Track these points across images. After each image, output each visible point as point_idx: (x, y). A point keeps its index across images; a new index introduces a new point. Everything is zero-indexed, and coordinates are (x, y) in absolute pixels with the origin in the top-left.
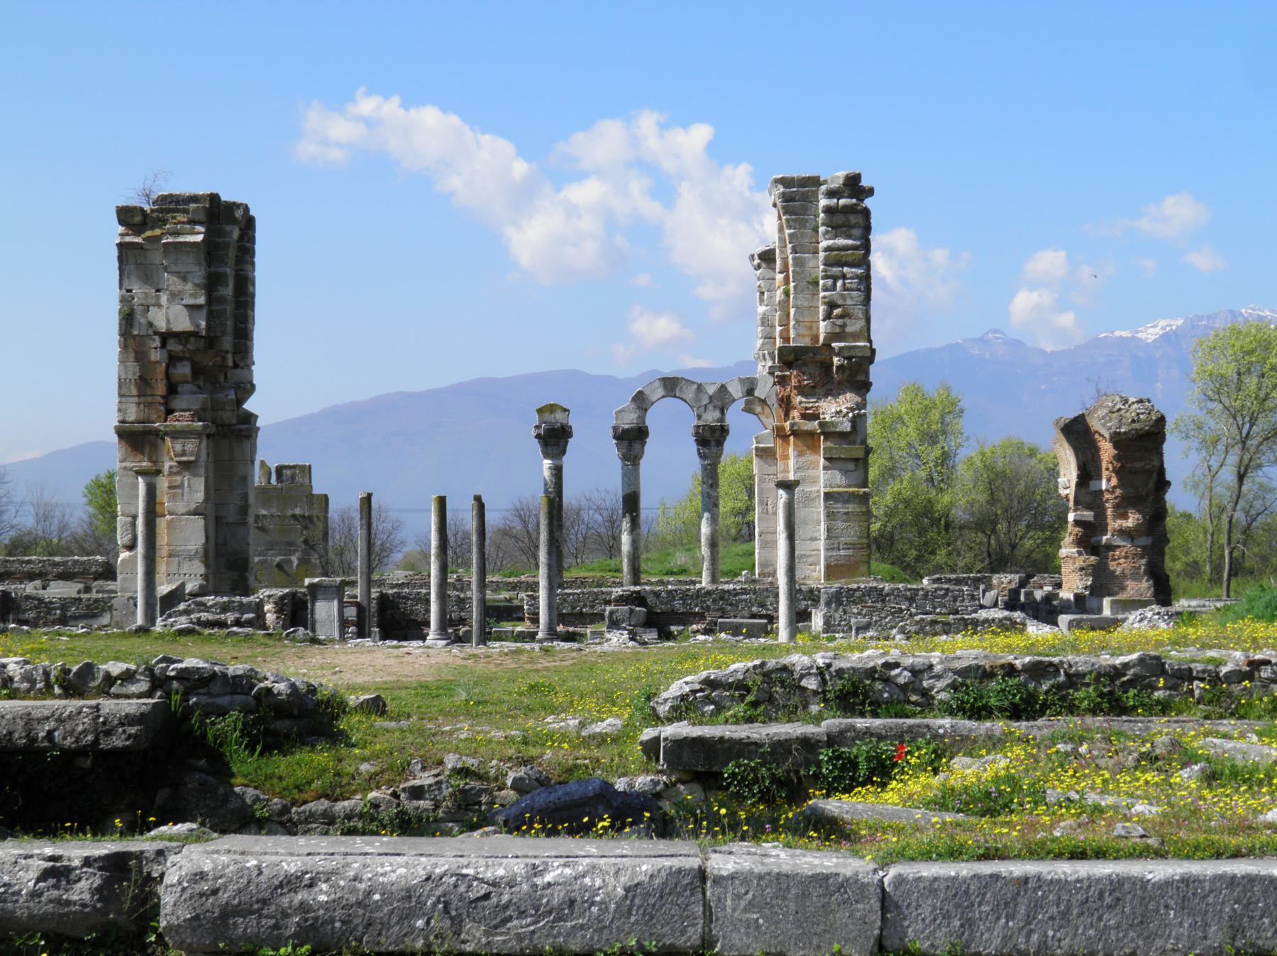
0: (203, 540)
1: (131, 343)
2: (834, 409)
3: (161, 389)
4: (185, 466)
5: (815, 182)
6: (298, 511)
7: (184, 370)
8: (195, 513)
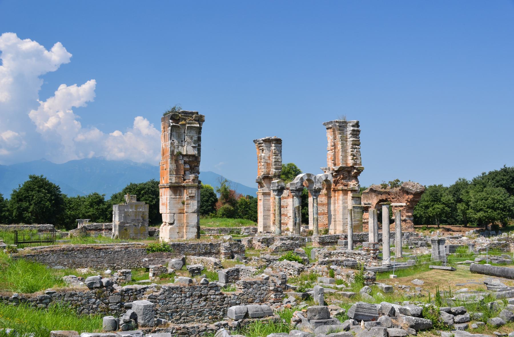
0: (197, 221)
1: (173, 157)
2: (352, 184)
3: (182, 173)
4: (192, 197)
5: (345, 123)
6: (141, 210)
7: (188, 167)
8: (194, 213)
